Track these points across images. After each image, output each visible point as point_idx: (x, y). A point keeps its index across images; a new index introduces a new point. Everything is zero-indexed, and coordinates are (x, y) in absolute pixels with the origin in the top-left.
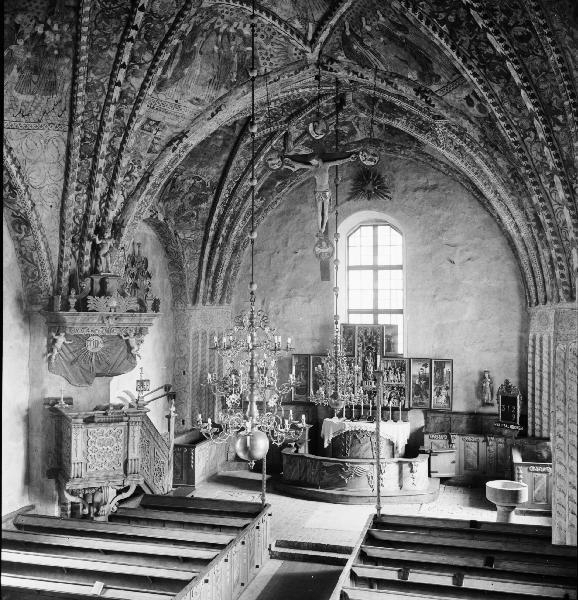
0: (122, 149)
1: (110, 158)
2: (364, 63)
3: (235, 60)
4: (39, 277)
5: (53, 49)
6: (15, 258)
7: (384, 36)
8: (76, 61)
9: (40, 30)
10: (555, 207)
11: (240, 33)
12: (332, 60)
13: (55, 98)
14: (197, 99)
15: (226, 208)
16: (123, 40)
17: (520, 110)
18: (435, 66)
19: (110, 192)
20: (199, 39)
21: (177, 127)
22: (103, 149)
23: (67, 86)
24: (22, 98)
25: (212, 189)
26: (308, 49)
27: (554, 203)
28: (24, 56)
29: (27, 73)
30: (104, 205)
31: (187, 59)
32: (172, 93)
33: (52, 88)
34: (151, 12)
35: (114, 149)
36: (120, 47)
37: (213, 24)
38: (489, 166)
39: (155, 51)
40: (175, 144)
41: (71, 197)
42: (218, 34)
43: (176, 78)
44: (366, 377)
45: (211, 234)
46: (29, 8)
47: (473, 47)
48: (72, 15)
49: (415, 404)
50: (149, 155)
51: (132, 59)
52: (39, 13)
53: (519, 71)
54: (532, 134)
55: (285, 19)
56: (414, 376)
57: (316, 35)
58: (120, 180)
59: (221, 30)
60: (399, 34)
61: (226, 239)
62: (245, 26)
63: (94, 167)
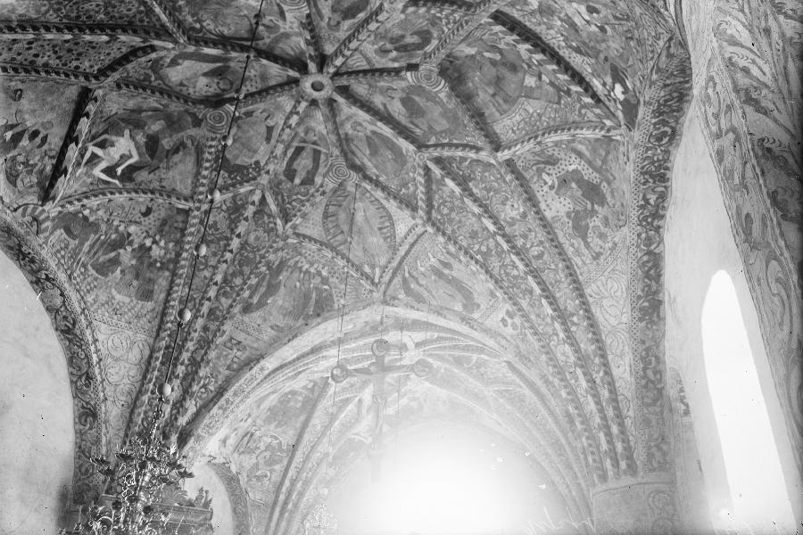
0: (202, 360)
1: (189, 368)
2: (419, 299)
3: (314, 296)
4: (92, 474)
5: (156, 261)
6: (72, 454)
7: (435, 274)
8: (174, 274)
9: (148, 242)
10: (582, 400)
11: (319, 273)
12: (394, 298)
13: (150, 305)
14: (278, 326)
15: (298, 473)
16: (219, 262)
18: (476, 296)
19: (184, 399)
20: (284, 273)
21: (257, 350)
22: (185, 356)
23: (163, 296)
24: (118, 297)
25: (288, 450)
26: (374, 289)
27: (580, 396)
28: (130, 260)
29: (129, 277)
30: (174, 412)
31: (272, 289)
32: (256, 316)
33: (146, 295)
34: (246, 242)
35: (195, 360)
36: (215, 267)
37: (297, 262)
38: (539, 429)
39: (246, 277)
40: (252, 364)
41: (145, 398)
42: (301, 272)
43: (261, 304)
45: (282, 497)
46: (143, 223)
47: (503, 272)
48: (178, 236)
50: (227, 372)
51: (225, 280)
52: (150, 229)
53: (538, 283)
54: (555, 338)
55: (357, 263)
57: (381, 277)
58: (195, 388)
59: (304, 269)
60: (446, 271)
61: (296, 506)
62: (323, 268)
63: (173, 373)
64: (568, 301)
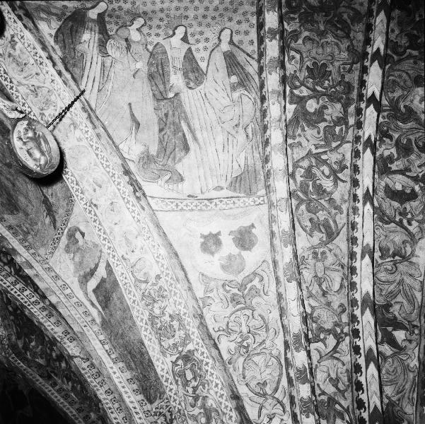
7: (150, 64)
17: (324, 294)
47: (305, 164)
54: (331, 341)
60: (177, 80)
64: (399, 298)
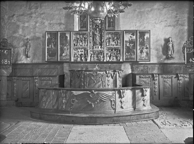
44: (95, 44)
49: (126, 59)
56: (126, 42)
